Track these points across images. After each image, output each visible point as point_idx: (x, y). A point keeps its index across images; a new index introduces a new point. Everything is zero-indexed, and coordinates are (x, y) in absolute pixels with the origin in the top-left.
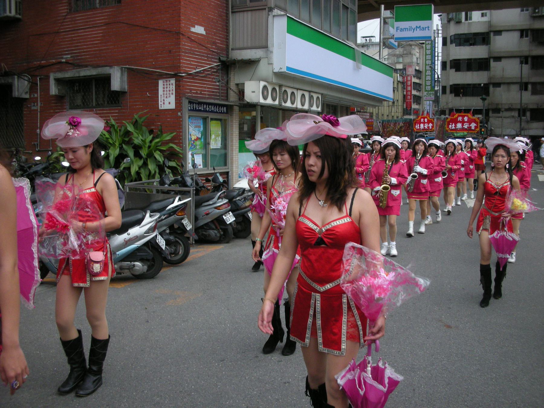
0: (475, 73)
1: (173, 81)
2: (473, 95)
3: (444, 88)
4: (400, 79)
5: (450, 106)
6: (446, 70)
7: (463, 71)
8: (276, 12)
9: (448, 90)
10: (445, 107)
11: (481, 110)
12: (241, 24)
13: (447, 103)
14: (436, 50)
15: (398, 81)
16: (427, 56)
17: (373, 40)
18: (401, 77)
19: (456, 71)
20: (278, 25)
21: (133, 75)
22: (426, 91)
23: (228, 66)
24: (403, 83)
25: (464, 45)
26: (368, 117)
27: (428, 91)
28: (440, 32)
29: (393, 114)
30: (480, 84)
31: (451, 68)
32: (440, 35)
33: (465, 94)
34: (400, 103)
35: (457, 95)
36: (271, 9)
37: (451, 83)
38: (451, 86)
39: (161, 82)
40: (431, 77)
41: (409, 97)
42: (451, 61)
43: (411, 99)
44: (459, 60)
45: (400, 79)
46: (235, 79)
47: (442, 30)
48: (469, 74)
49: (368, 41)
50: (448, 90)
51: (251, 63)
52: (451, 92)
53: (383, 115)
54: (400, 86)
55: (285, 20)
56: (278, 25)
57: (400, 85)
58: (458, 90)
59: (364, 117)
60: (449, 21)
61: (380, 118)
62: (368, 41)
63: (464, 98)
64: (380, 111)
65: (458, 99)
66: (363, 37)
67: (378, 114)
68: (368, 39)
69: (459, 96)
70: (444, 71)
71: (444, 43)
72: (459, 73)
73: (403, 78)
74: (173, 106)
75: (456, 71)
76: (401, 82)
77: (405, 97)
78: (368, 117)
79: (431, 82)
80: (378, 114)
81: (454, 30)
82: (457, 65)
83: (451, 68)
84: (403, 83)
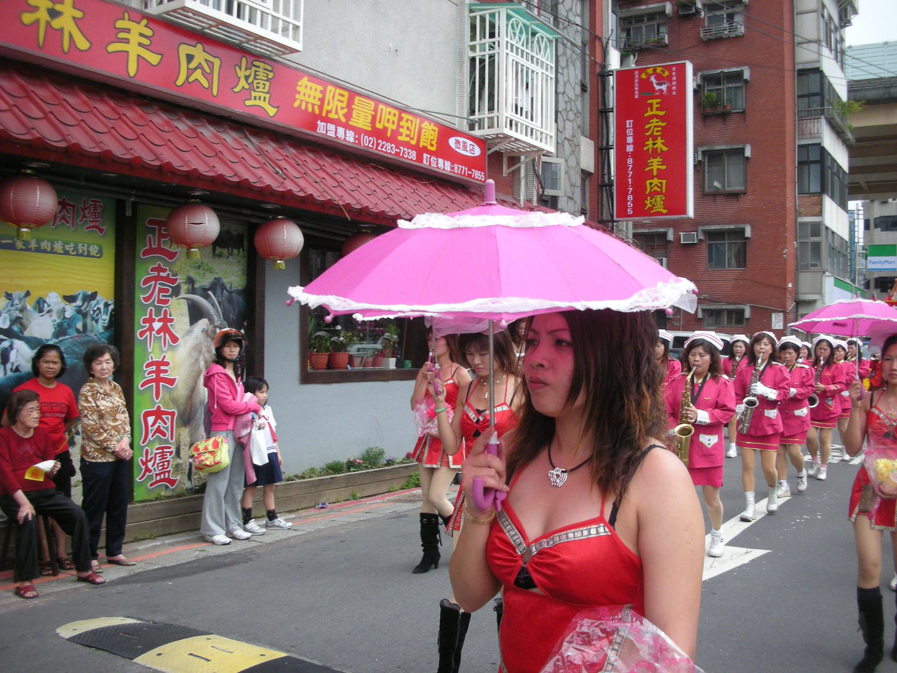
1: (781, 314)
8: (827, 273)
9: (872, 285)
12: (806, 278)
20: (829, 282)
21: (753, 309)
23: (799, 303)
25: (891, 230)
28: (861, 212)
32: (861, 217)
36: (824, 272)
39: (773, 315)
47: (865, 211)
51: (812, 302)
52: (876, 287)
55: (832, 279)
56: (829, 282)
60: (872, 201)
71: (867, 226)
74: (781, 328)
81: (879, 211)
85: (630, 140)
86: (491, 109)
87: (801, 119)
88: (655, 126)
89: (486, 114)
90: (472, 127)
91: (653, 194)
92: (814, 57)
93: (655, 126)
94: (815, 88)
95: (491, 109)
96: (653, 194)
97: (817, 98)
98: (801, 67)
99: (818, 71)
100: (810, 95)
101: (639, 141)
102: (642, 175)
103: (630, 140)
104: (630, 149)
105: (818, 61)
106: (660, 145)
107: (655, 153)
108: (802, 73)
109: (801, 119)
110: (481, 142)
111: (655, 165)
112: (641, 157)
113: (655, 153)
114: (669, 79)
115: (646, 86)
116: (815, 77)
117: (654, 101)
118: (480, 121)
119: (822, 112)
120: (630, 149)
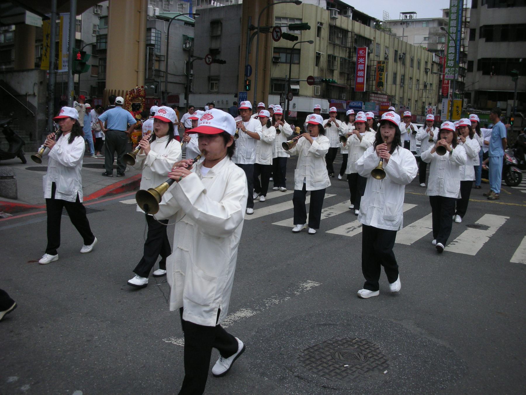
0: (512, 44)
2: (508, 73)
3: (471, 64)
4: (436, 59)
5: (477, 87)
6: (474, 40)
7: (496, 41)
9: (475, 67)
10: (471, 89)
11: (513, 93)
13: (473, 83)
14: (464, 15)
15: (434, 62)
16: (452, 22)
17: (414, 16)
18: (438, 58)
19: (487, 41)
22: (448, 67)
24: (439, 64)
26: (385, 100)
27: (451, 67)
29: (424, 100)
30: (518, 59)
31: (480, 37)
33: (497, 72)
34: (434, 87)
35: (486, 73)
37: (479, 57)
38: (479, 61)
40: (456, 49)
41: (446, 82)
42: (481, 28)
43: (448, 83)
44: (492, 26)
45: (436, 59)
48: (504, 45)
49: (408, 18)
50: (475, 67)
52: (479, 69)
53: (409, 100)
54: (436, 69)
57: (435, 66)
58: (488, 66)
59: (380, 99)
61: (405, 103)
62: (408, 18)
63: (495, 78)
64: (406, 95)
65: (487, 77)
66: (403, 13)
67: (402, 98)
68: (408, 15)
69: (489, 74)
70: (471, 42)
72: (491, 45)
73: (441, 58)
75: (487, 41)
76: (437, 63)
77: (441, 82)
78: (385, 100)
79: (455, 56)
80: (402, 98)
82: (489, 33)
83: (480, 37)
84: (439, 64)
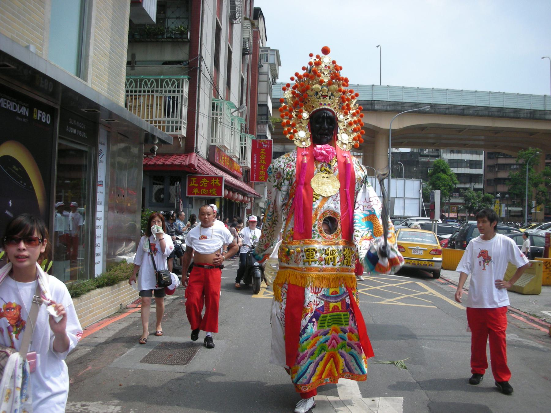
46: (257, 201)
85: (255, 159)
86: (244, 159)
87: (258, 124)
88: (263, 156)
89: (243, 161)
90: (239, 163)
91: (261, 175)
92: (265, 100)
93: (263, 156)
94: (264, 112)
95: (244, 159)
96: (261, 175)
97: (265, 117)
98: (259, 103)
99: (267, 106)
100: (262, 115)
101: (258, 160)
102: (258, 170)
103: (255, 159)
104: (255, 162)
105: (267, 102)
106: (264, 162)
107: (262, 164)
108: (260, 105)
109: (258, 124)
110: (243, 167)
111: (262, 167)
112: (258, 165)
113: (262, 164)
114: (267, 144)
115: (261, 145)
116: (264, 108)
117: (263, 150)
118: (242, 163)
119: (267, 122)
120: (255, 162)
